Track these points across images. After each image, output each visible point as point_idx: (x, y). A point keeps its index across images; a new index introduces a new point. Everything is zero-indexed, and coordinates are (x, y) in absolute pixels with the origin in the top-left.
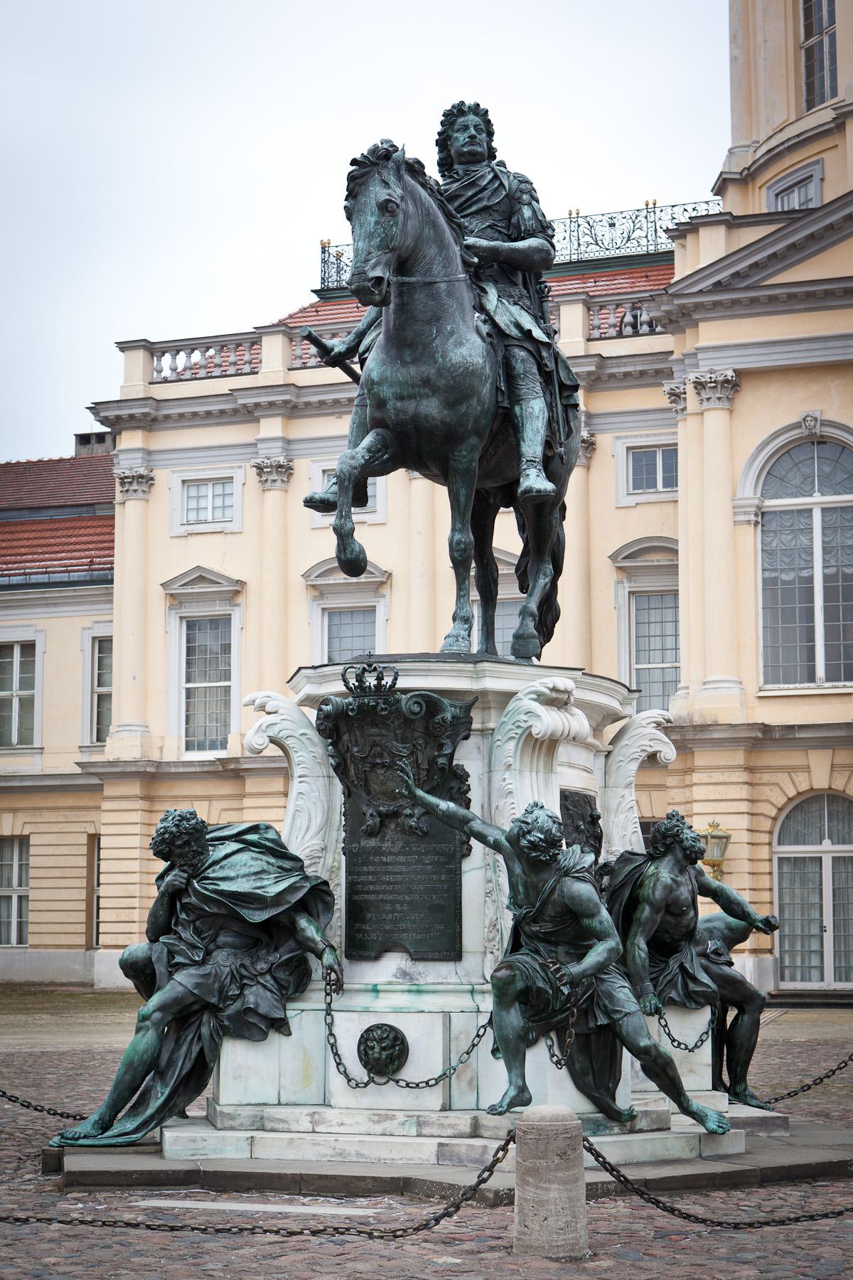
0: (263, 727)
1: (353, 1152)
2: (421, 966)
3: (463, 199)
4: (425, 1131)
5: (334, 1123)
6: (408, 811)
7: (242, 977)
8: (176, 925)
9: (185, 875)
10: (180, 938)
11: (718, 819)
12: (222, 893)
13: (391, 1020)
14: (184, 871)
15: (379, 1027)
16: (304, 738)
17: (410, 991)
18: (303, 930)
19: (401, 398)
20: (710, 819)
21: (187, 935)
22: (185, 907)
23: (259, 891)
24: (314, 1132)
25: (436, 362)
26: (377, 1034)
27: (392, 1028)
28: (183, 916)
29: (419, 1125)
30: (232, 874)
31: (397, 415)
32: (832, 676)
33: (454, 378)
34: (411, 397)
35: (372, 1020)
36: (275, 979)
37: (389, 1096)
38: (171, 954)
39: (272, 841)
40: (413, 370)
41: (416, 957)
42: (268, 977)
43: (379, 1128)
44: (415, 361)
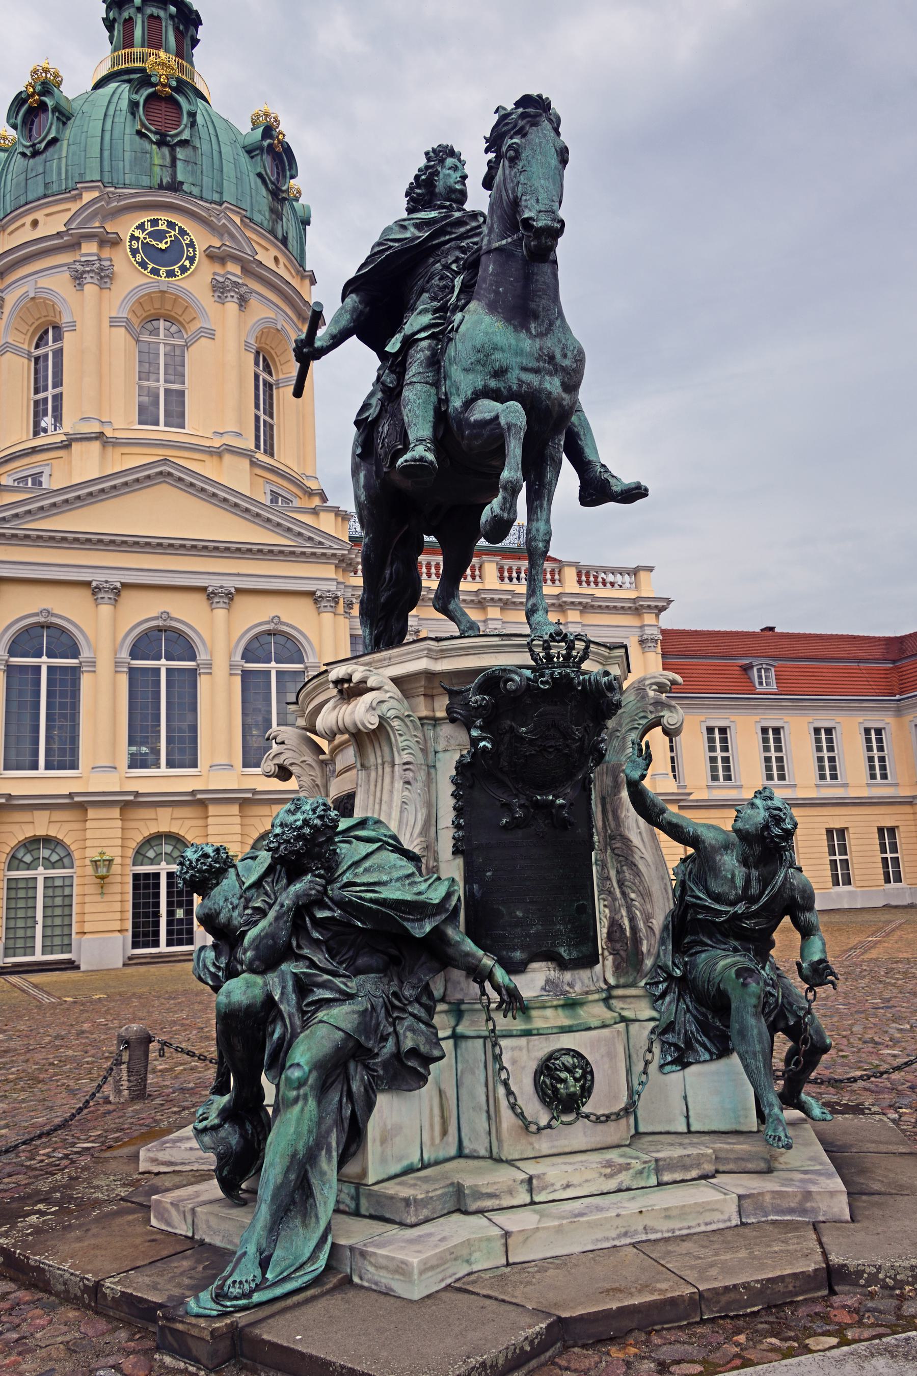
0: (374, 704)
1: (640, 1228)
2: (568, 976)
3: (468, 227)
4: (667, 1177)
5: (558, 1186)
6: (560, 801)
7: (395, 1007)
8: (299, 947)
9: (323, 882)
10: (313, 965)
11: (105, 850)
12: (384, 902)
13: (567, 1041)
14: (319, 876)
15: (568, 1051)
16: (407, 720)
17: (563, 1006)
18: (458, 943)
19: (525, 369)
20: (100, 850)
21: (320, 958)
22: (319, 924)
23: (422, 898)
24: (533, 1203)
25: (559, 341)
26: (568, 1060)
27: (577, 1054)
28: (316, 935)
29: (658, 1171)
30: (385, 878)
31: (520, 386)
32: (47, 768)
33: (576, 361)
34: (536, 371)
35: (542, 1048)
36: (421, 1004)
37: (578, 1134)
38: (302, 987)
39: (391, 837)
40: (538, 343)
41: (563, 965)
42: (417, 1006)
43: (612, 1184)
44: (540, 335)
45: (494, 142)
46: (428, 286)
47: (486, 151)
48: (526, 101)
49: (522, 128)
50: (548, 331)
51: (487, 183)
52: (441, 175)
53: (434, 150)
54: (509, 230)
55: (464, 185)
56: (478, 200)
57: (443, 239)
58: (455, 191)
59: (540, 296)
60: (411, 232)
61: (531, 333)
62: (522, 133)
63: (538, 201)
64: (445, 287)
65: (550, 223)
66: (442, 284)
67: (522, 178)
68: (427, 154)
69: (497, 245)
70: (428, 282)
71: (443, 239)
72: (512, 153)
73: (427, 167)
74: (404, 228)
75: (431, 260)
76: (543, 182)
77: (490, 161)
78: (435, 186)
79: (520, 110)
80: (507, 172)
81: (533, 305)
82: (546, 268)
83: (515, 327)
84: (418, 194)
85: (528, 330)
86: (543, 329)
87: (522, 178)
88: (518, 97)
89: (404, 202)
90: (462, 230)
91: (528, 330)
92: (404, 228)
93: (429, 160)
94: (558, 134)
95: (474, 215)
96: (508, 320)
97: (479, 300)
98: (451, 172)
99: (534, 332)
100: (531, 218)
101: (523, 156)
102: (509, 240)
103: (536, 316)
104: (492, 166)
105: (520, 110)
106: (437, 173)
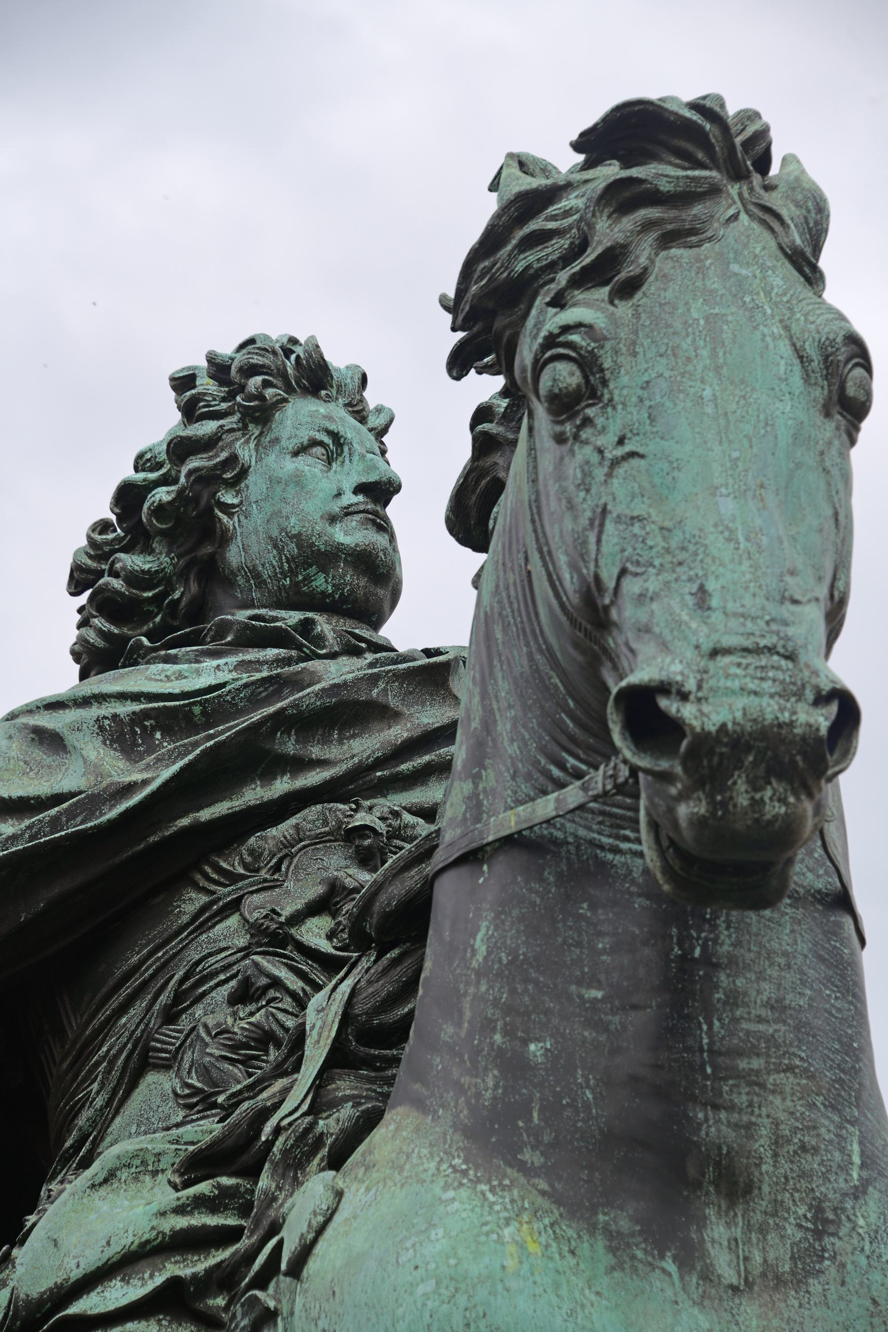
3: (398, 733)
45: (488, 314)
46: (172, 1035)
47: (459, 364)
48: (628, 131)
49: (613, 257)
50: (809, 1260)
51: (469, 518)
52: (255, 483)
53: (218, 368)
54: (572, 744)
55: (383, 526)
56: (437, 598)
57: (254, 794)
58: (327, 557)
59: (754, 1081)
60: (92, 766)
61: (707, 1276)
62: (609, 272)
63: (702, 595)
64: (264, 1039)
65: (771, 709)
66: (243, 1022)
67: (620, 493)
68: (183, 383)
69: (507, 821)
70: (170, 1016)
71: (254, 794)
72: (564, 375)
73: (180, 448)
74: (51, 741)
75: (192, 902)
76: (728, 506)
77: (482, 414)
78: (225, 539)
79: (611, 171)
80: (546, 463)
81: (715, 1128)
82: (784, 932)
83: (617, 1243)
84: (135, 579)
85: (691, 1258)
86: (779, 1252)
87: (620, 493)
88: (591, 115)
89: (62, 617)
90: (365, 746)
91: (691, 1258)
92: (51, 741)
93: (190, 411)
94: (812, 276)
95: (432, 674)
96: (577, 1206)
97: (420, 1105)
98: (310, 466)
99: (725, 1268)
100: (665, 688)
101: (623, 384)
102: (573, 795)
103: (734, 1184)
104: (490, 437)
105: (611, 171)
106: (235, 473)
